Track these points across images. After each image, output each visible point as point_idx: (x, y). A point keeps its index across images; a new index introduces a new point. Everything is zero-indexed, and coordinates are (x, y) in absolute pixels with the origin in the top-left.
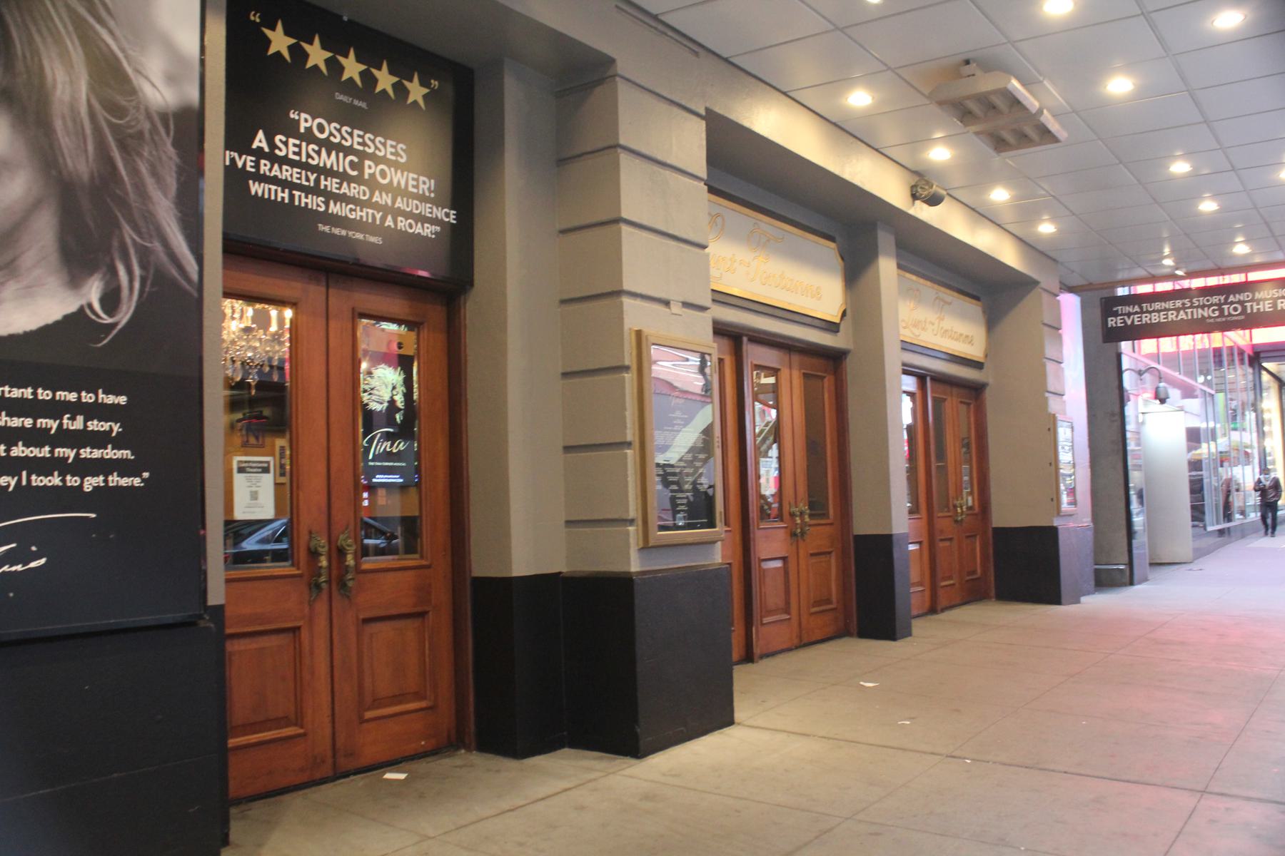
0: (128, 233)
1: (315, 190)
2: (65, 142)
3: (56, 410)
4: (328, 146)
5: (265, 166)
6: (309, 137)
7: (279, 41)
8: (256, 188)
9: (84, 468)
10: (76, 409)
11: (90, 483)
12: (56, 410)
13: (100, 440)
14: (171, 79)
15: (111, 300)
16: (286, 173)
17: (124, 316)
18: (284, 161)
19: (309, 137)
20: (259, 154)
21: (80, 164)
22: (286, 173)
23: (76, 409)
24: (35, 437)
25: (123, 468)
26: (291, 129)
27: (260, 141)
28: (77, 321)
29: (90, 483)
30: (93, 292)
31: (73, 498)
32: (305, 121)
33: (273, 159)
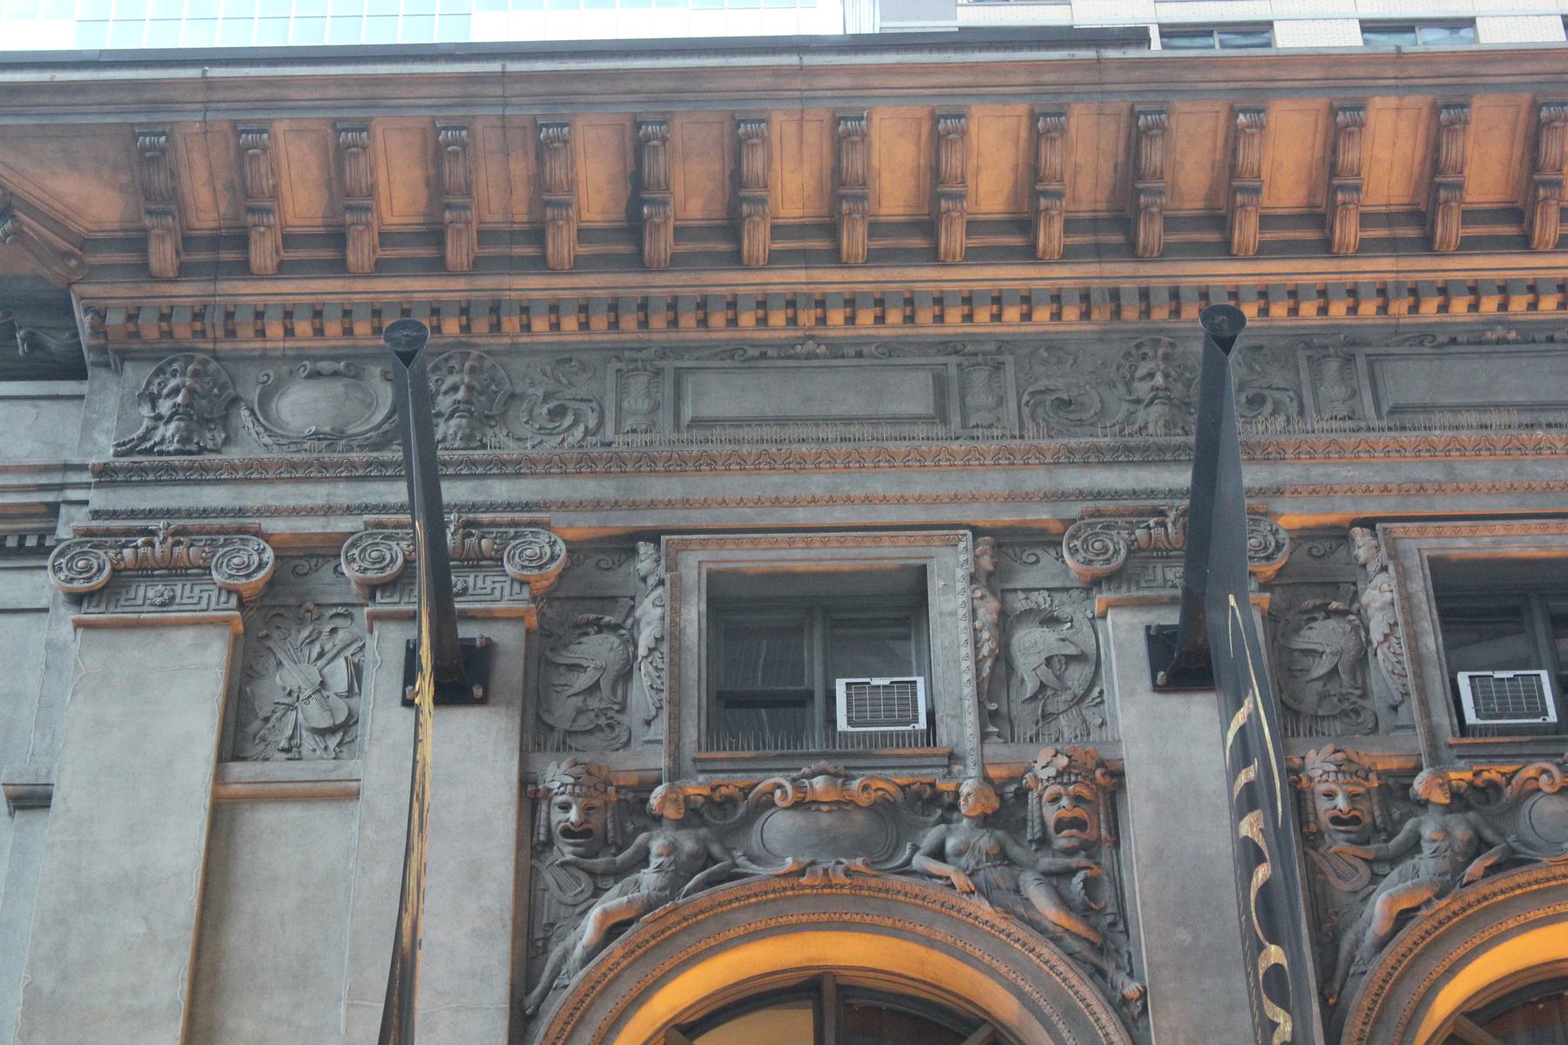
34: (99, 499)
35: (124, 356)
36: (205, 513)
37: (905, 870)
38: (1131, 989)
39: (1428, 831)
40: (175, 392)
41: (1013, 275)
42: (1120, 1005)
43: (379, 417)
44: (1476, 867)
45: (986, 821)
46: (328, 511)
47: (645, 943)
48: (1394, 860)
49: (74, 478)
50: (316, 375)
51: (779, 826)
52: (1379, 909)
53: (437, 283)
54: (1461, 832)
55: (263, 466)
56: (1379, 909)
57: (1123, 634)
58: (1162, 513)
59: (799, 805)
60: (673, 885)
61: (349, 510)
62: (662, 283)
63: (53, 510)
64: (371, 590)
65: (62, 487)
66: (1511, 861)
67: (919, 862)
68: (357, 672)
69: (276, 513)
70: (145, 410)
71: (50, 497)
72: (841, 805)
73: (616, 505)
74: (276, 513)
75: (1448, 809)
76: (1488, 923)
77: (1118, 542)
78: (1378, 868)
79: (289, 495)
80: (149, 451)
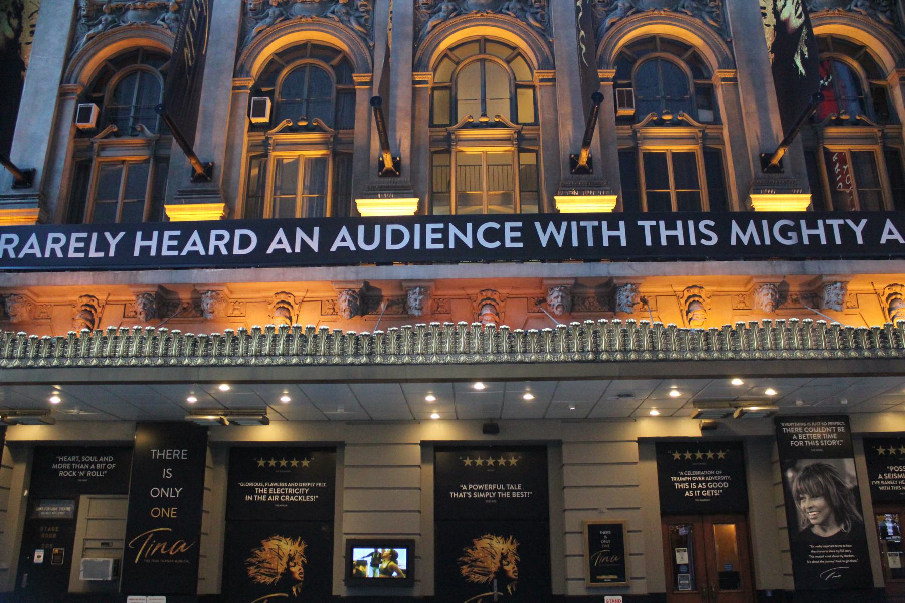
0: (847, 515)
1: (898, 485)
2: (833, 500)
3: (838, 549)
4: (900, 473)
5: (883, 482)
6: (894, 472)
7: (881, 451)
8: (881, 488)
9: (845, 559)
10: (842, 548)
11: (847, 562)
12: (838, 549)
13: (848, 554)
14: (851, 482)
15: (846, 528)
16: (889, 482)
17: (849, 530)
18: (887, 480)
19: (894, 472)
20: (881, 480)
21: (836, 504)
22: (889, 482)
23: (842, 548)
24: (835, 554)
25: (853, 559)
26: (888, 472)
27: (880, 477)
28: (840, 533)
29: (847, 562)
30: (842, 527)
31: (844, 564)
32: (892, 468)
33: (884, 480)
37: (156, 24)
39: (270, 12)
44: (452, 15)
45: (175, 12)
47: (98, 41)
48: (262, 19)
51: (130, 14)
52: (430, 24)
54: (277, 12)
56: (430, 24)
59: (135, 9)
60: (105, 28)
66: (287, 18)
67: (159, 22)
72: (144, 8)
75: (276, 7)
76: (455, 28)
78: (257, 21)
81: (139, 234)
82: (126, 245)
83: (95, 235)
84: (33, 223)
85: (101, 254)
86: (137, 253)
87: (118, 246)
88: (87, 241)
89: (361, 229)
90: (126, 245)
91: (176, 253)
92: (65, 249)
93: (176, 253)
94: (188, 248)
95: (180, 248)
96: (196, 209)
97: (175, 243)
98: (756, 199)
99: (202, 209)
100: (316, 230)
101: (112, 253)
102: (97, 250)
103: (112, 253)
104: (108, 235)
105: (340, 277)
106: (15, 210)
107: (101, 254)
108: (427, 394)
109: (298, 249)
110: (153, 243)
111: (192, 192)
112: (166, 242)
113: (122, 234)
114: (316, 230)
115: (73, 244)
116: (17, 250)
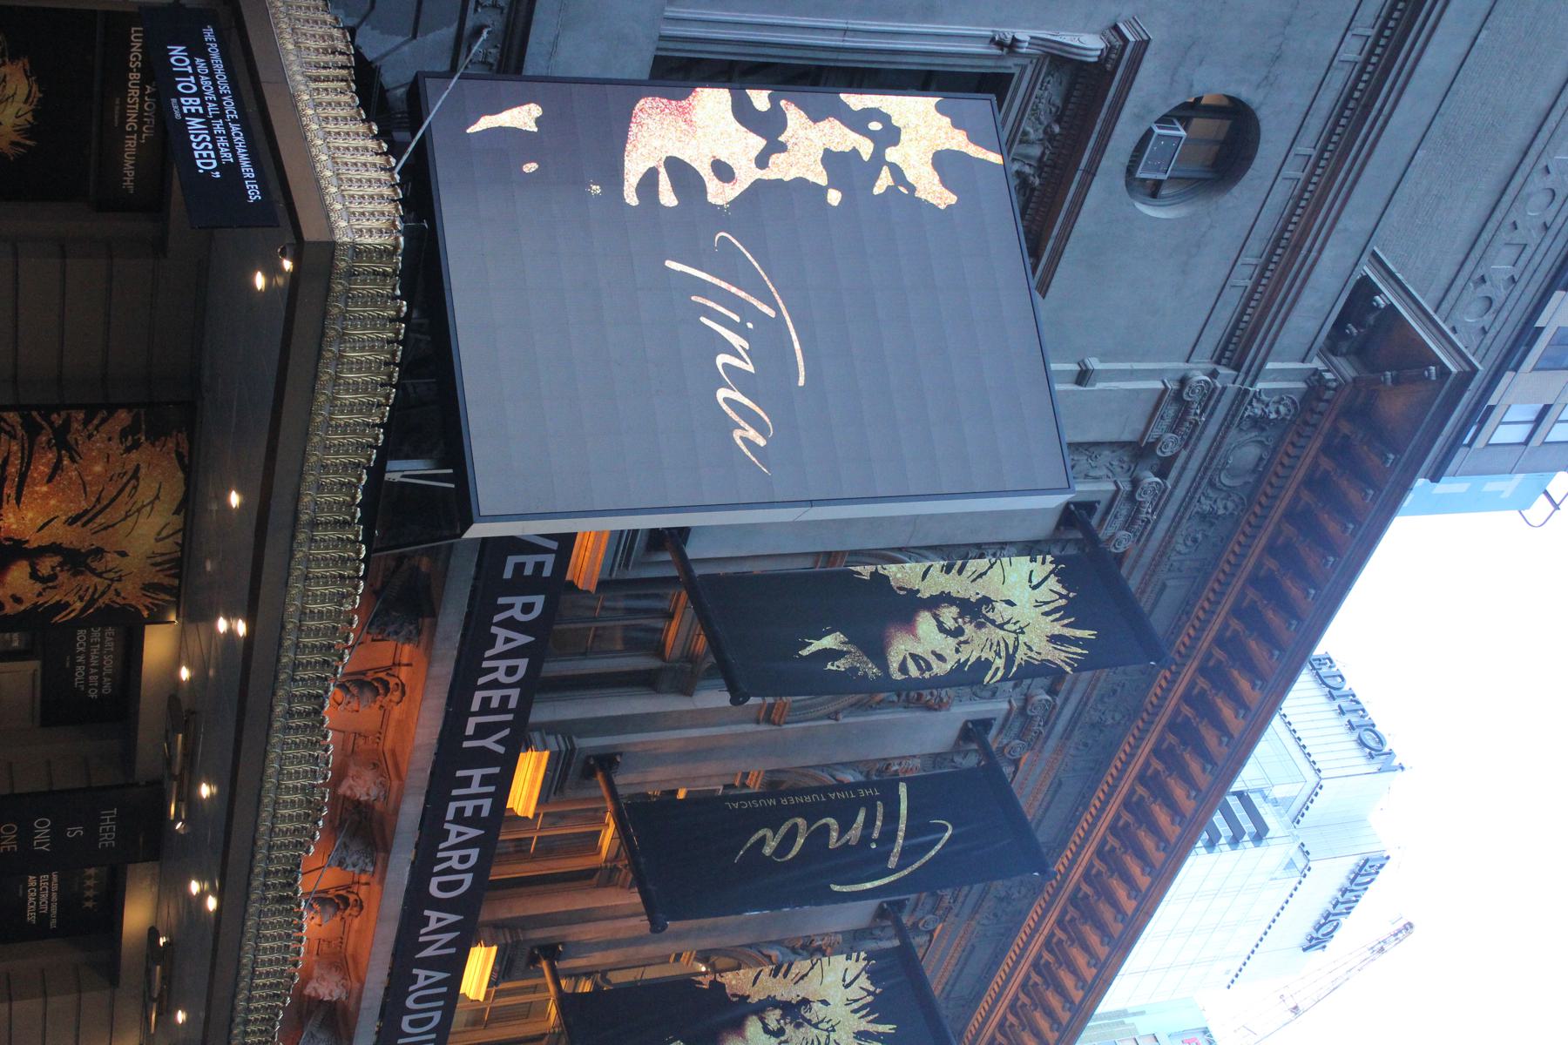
34: (1233, 388)
35: (1311, 388)
36: (1199, 439)
38: (840, 716)
40: (1278, 412)
41: (1180, 689)
42: (837, 713)
43: (1226, 481)
46: (1184, 468)
49: (1249, 379)
50: (1261, 459)
53: (1280, 511)
55: (1218, 448)
57: (997, 708)
58: (1046, 723)
61: (1180, 475)
62: (1238, 584)
63: (1237, 368)
64: (1135, 483)
65: (1247, 374)
68: (1097, 478)
69: (1189, 457)
70: (1276, 398)
71: (1244, 369)
73: (1136, 562)
74: (1189, 457)
77: (1036, 713)
79: (1194, 464)
80: (1250, 403)
81: (496, 770)
82: (482, 757)
83: (510, 717)
84: (568, 577)
85: (470, 730)
86: (459, 773)
87: (483, 748)
88: (503, 708)
89: (444, 989)
90: (482, 757)
91: (450, 815)
92: (495, 684)
93: (450, 815)
94: (454, 829)
95: (459, 818)
96: (532, 785)
97: (468, 813)
98: (488, 955)
99: (530, 796)
100: (453, 950)
101: (466, 744)
102: (477, 725)
103: (466, 744)
104: (506, 732)
105: (367, 994)
106: (601, 556)
107: (470, 730)
108: (209, 784)
109: (421, 939)
110: (475, 788)
111: (567, 764)
112: (469, 806)
113: (501, 749)
114: (453, 950)
115: (496, 696)
116: (510, 624)
